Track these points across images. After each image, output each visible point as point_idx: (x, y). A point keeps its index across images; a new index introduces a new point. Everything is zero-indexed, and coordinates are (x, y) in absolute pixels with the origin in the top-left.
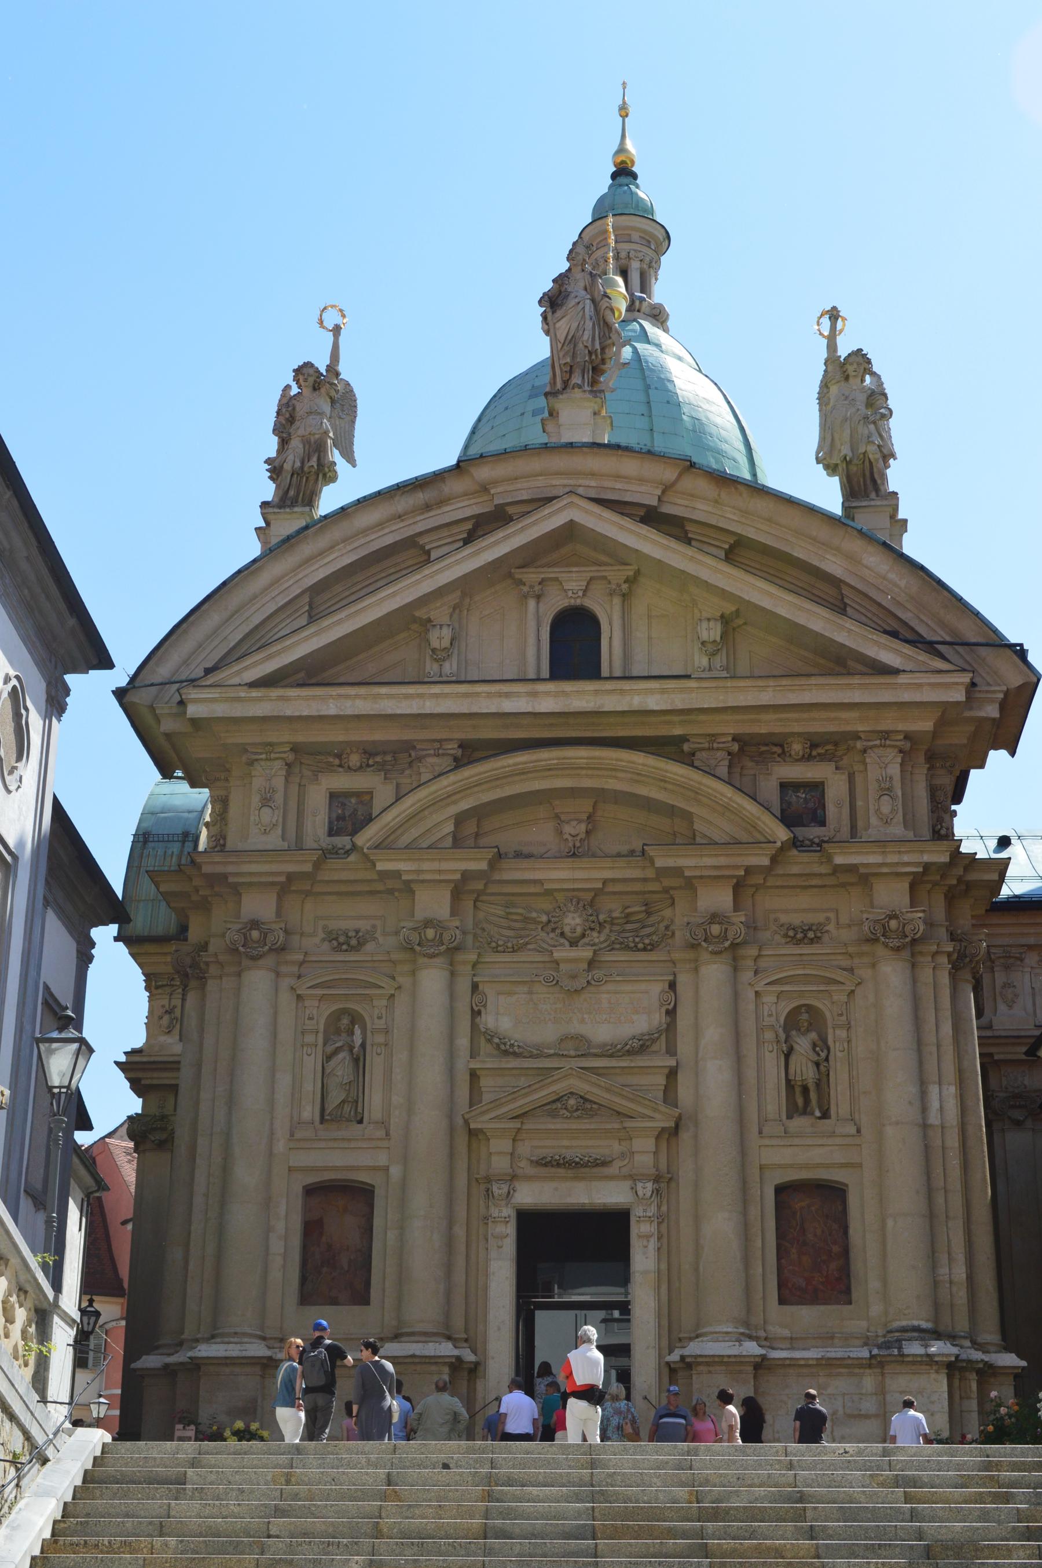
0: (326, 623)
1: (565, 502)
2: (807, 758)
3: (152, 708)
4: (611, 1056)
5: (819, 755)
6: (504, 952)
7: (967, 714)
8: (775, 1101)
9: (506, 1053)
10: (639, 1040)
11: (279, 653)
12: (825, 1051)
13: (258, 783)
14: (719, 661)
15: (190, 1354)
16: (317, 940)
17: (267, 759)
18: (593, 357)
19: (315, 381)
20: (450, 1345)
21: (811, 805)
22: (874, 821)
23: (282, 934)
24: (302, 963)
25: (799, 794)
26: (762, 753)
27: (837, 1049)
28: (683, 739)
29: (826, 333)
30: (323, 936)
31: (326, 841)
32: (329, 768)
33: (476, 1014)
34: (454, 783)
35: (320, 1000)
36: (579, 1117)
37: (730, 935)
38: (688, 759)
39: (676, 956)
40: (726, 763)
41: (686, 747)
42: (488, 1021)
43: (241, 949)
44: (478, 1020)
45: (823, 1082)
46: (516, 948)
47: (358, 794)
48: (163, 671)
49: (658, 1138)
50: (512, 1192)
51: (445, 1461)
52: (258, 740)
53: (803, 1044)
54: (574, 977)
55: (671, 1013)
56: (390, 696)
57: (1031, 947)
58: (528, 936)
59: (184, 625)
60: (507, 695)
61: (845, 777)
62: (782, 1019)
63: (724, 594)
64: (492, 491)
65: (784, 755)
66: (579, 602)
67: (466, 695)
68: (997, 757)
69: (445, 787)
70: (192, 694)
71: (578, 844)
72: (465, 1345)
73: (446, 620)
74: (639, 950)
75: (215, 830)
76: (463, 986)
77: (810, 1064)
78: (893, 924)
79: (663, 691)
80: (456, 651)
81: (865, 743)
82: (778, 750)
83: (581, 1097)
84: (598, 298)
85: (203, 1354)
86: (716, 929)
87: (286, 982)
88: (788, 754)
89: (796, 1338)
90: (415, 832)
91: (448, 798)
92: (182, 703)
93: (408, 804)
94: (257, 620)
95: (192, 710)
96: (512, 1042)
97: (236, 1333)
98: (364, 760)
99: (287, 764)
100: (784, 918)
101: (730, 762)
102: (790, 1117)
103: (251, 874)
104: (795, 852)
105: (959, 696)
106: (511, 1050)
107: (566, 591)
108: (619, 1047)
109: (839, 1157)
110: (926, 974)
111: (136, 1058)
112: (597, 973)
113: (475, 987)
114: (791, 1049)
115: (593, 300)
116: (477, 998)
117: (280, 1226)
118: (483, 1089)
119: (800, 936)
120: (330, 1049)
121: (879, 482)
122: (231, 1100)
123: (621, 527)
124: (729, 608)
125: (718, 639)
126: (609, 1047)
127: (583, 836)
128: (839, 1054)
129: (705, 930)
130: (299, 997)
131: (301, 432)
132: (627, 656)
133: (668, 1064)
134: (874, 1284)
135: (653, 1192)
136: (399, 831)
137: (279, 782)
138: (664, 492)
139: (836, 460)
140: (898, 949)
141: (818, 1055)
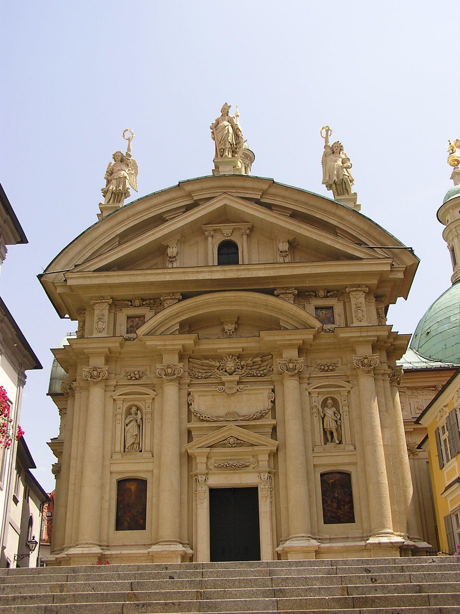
0: (124, 246)
1: (223, 197)
2: (327, 297)
3: (53, 283)
4: (248, 420)
5: (331, 295)
6: (201, 379)
7: (391, 277)
8: (319, 436)
9: (203, 420)
10: (260, 413)
11: (105, 258)
12: (339, 416)
13: (97, 312)
14: (287, 260)
15: (66, 553)
16: (122, 376)
17: (101, 303)
18: (232, 146)
19: (122, 159)
20: (181, 545)
21: (328, 316)
22: (355, 320)
23: (106, 372)
24: (116, 386)
25: (323, 312)
26: (307, 295)
27: (344, 415)
28: (275, 289)
29: (324, 136)
30: (125, 374)
31: (126, 336)
32: (127, 306)
33: (189, 405)
34: (179, 308)
35: (123, 401)
36: (235, 447)
37: (297, 367)
38: (277, 296)
39: (274, 379)
40: (293, 299)
41: (275, 292)
42: (195, 407)
43: (89, 379)
44: (190, 407)
45: (339, 428)
46: (206, 377)
47: (139, 317)
48: (58, 268)
49: (269, 455)
50: (207, 479)
51: (171, 575)
52: (97, 295)
53: (330, 412)
54: (231, 388)
55: (273, 402)
56: (151, 274)
57: (408, 388)
58: (212, 372)
59: (67, 249)
60: (201, 272)
61: (342, 303)
62: (320, 403)
63: (289, 231)
64: (193, 195)
65: (316, 296)
66: (229, 238)
67: (184, 272)
68: (400, 300)
69: (175, 310)
70: (69, 275)
71: (231, 333)
72: (188, 546)
73: (175, 245)
74: (258, 377)
75: (79, 334)
76: (185, 392)
77: (334, 422)
78: (366, 361)
79: (265, 269)
80: (179, 258)
81: (350, 289)
82: (314, 294)
83: (236, 438)
84: (234, 126)
85: (73, 553)
86: (291, 366)
87: (109, 394)
88: (318, 295)
89: (332, 539)
90: (163, 329)
91: (177, 315)
92: (66, 280)
93: (160, 317)
94: (96, 248)
95: (69, 282)
96: (205, 415)
97: (87, 543)
98: (141, 302)
99: (109, 304)
100: (319, 362)
101: (294, 298)
102: (325, 444)
103: (94, 348)
104: (323, 333)
105: (388, 268)
106: (205, 419)
107: (223, 233)
108: (251, 416)
109: (347, 460)
110: (381, 383)
111: (54, 441)
112: (241, 386)
113: (189, 394)
114: (325, 415)
115: (232, 127)
116: (190, 398)
117: (107, 497)
118: (193, 436)
119: (326, 368)
120: (127, 421)
121: (348, 190)
122: (84, 444)
123: (246, 206)
124: (291, 238)
125: (287, 250)
126: (247, 417)
127: (234, 330)
128: (345, 417)
129: (287, 366)
130: (114, 400)
131: (115, 177)
132: (249, 259)
133: (273, 423)
134: (364, 514)
135: (268, 478)
136: (156, 329)
137: (106, 312)
138: (263, 194)
139: (331, 182)
140: (369, 372)
141: (337, 417)
